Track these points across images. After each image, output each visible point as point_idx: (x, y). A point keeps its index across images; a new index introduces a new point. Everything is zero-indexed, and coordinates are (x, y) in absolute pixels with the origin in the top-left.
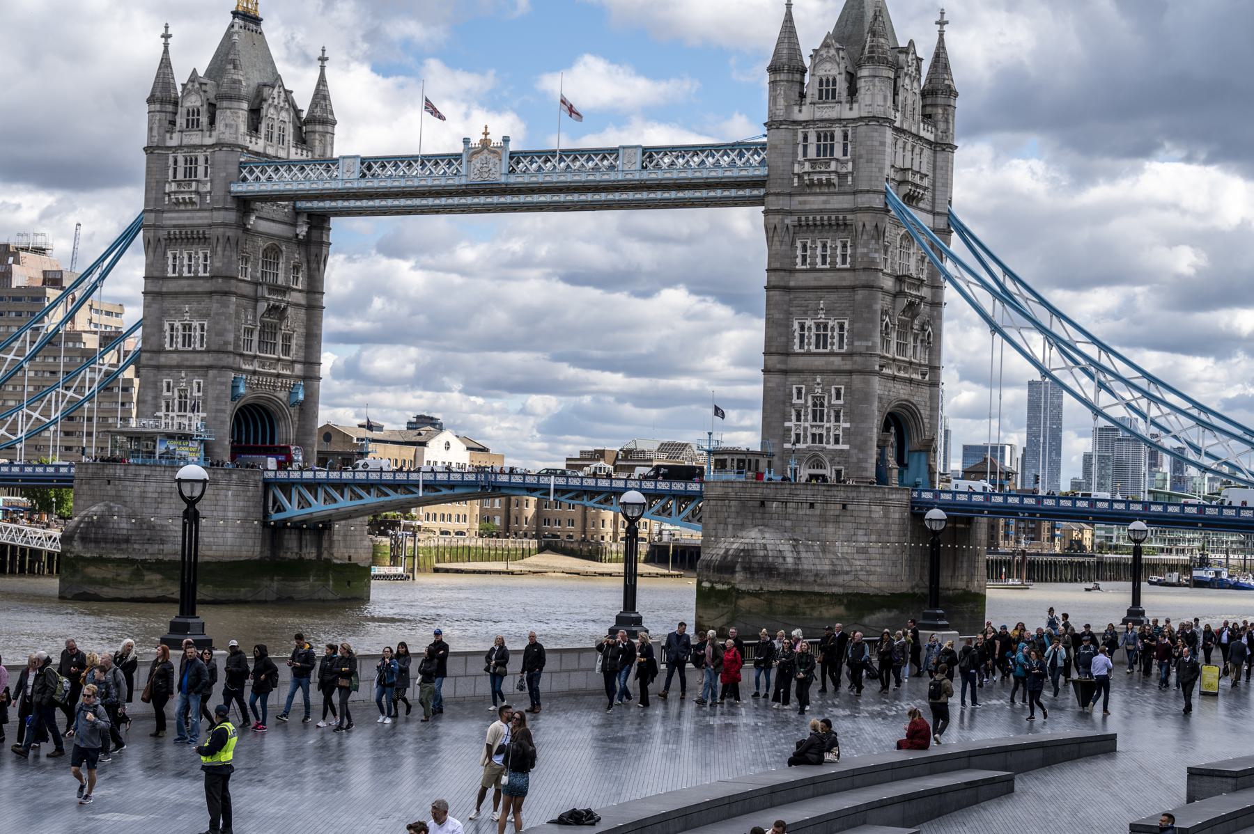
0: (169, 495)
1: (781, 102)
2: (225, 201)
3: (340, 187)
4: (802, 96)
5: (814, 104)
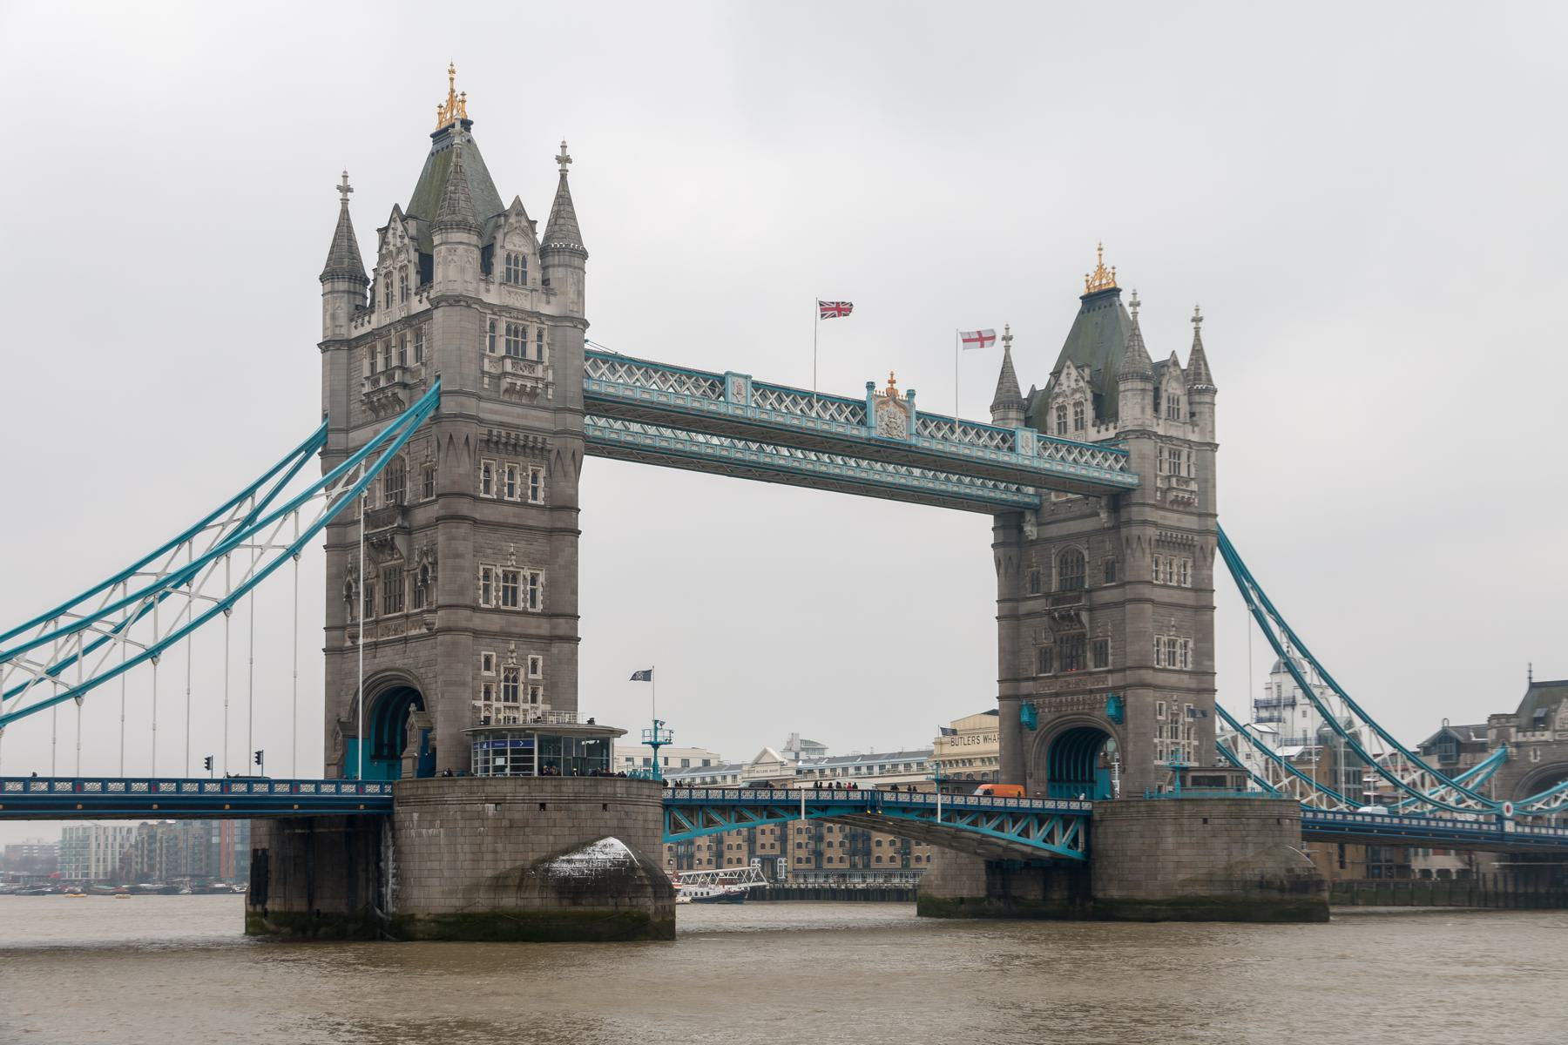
1: (1149, 411)
3: (730, 411)
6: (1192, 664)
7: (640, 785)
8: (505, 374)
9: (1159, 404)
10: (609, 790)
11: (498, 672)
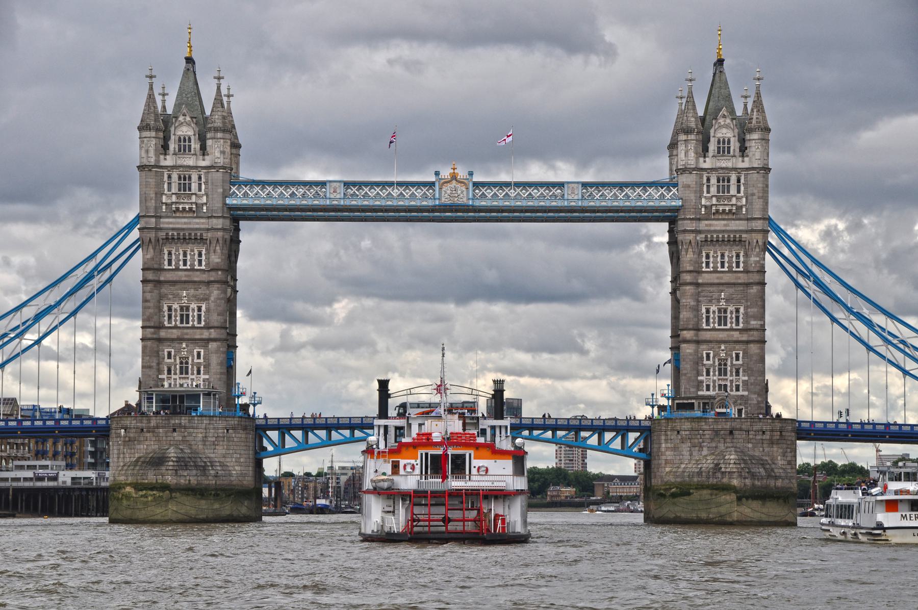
0: (222, 439)
1: (692, 154)
2: (223, 212)
3: (328, 202)
4: (706, 150)
5: (716, 157)
6: (743, 323)
7: (200, 418)
8: (173, 203)
9: (708, 148)
10: (177, 421)
11: (175, 359)
